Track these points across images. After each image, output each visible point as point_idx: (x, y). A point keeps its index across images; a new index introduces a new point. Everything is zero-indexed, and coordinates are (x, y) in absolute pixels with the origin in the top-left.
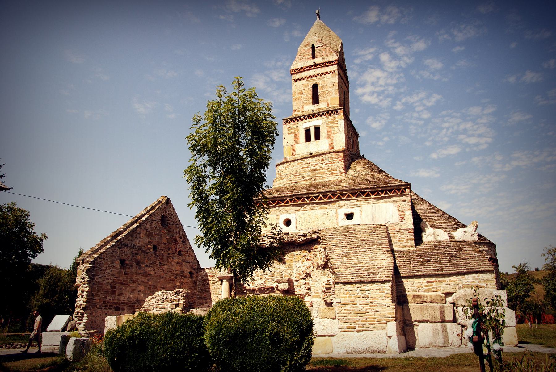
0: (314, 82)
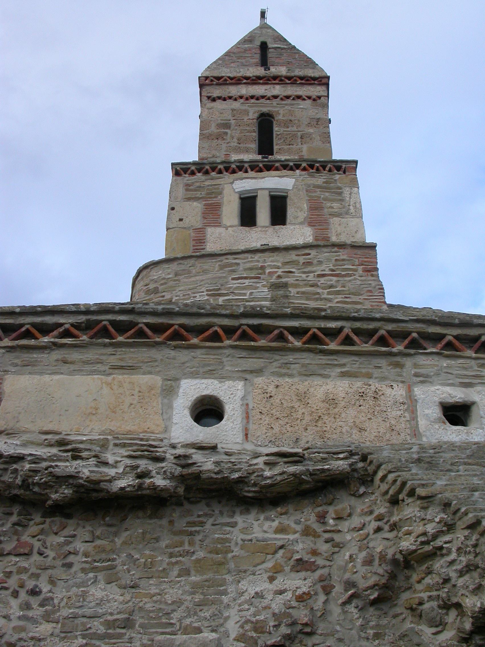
0: (265, 110)
